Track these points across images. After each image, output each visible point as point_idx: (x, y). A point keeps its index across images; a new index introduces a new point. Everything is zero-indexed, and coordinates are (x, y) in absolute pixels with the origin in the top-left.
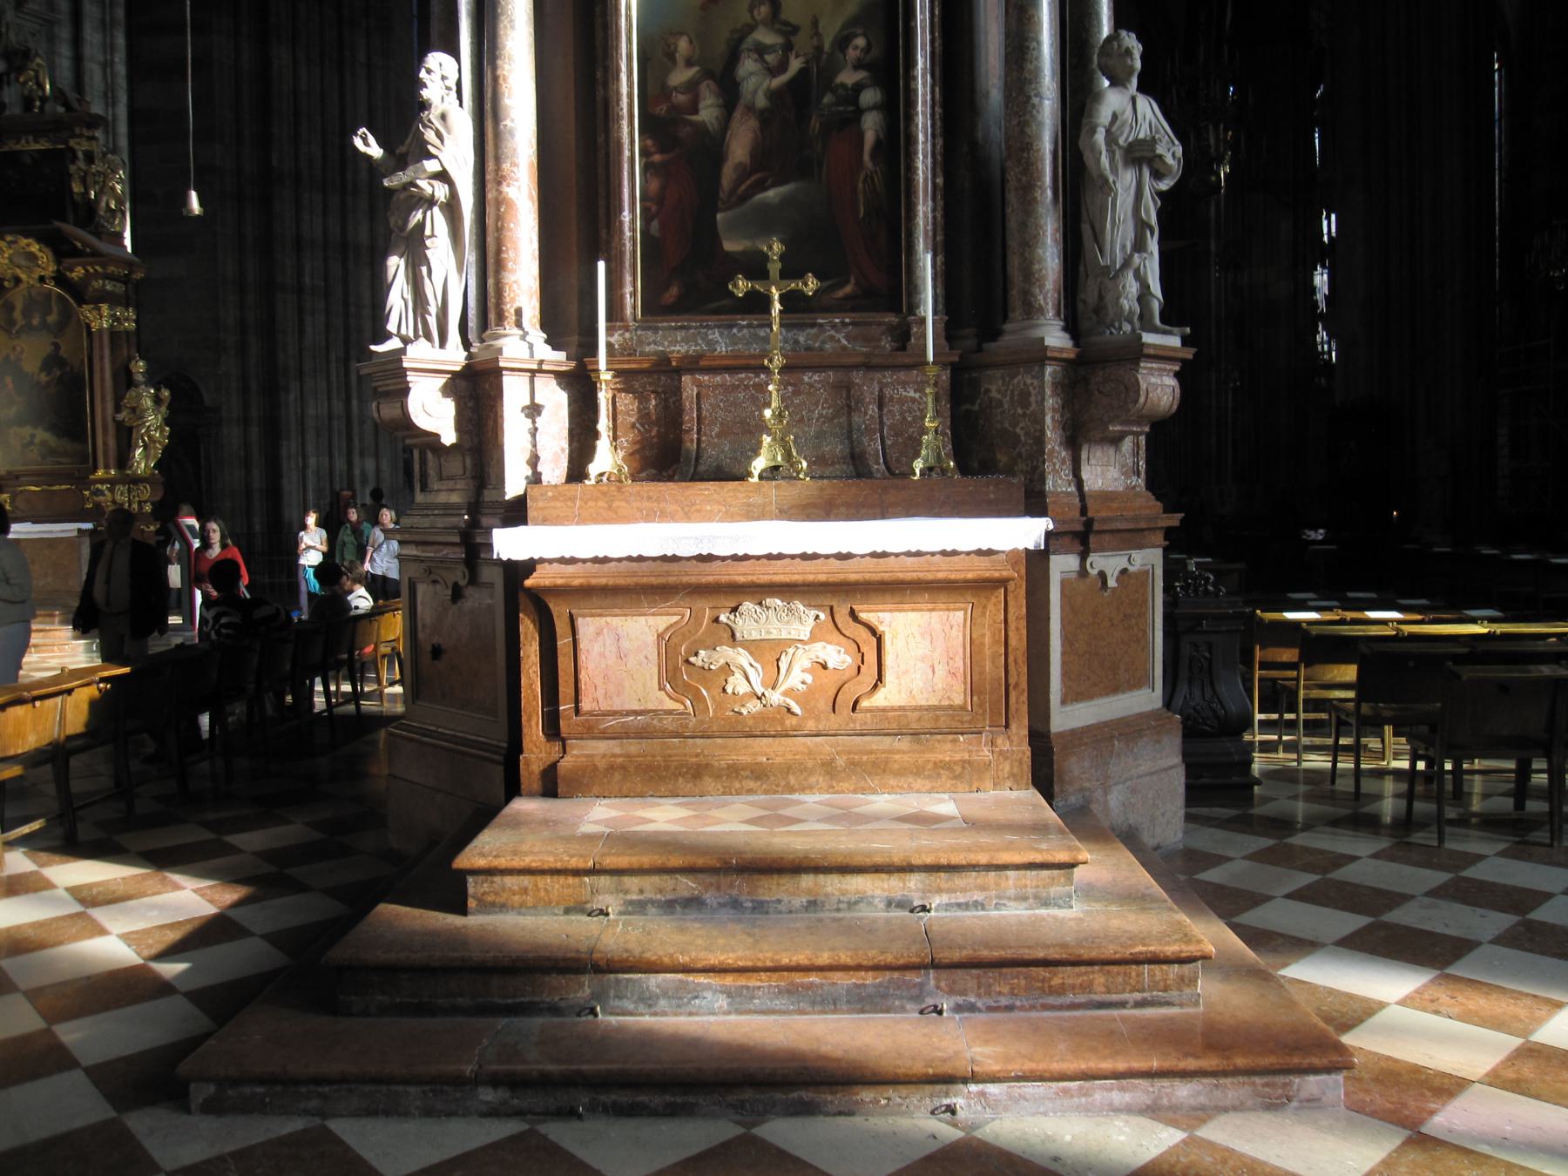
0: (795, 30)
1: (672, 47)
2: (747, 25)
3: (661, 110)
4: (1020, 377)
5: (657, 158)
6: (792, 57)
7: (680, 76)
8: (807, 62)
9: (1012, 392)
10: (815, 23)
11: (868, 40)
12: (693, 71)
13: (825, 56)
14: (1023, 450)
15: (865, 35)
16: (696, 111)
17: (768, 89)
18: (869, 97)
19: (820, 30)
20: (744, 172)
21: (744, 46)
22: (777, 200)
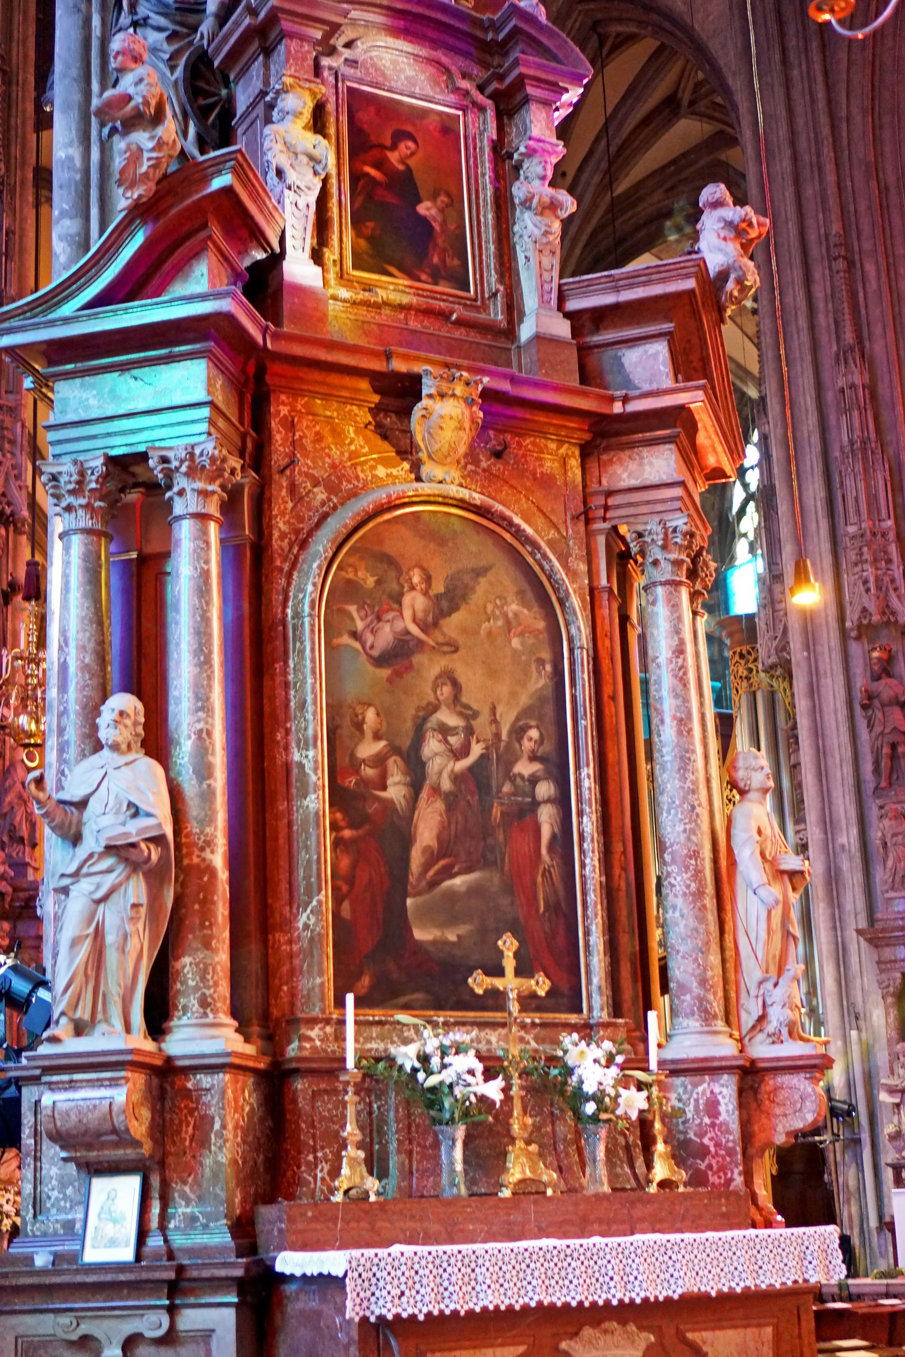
0: (475, 715)
1: (360, 717)
2: (429, 704)
3: (351, 782)
4: (705, 1085)
5: (347, 833)
6: (474, 741)
7: (368, 749)
8: (487, 748)
9: (697, 1101)
10: (493, 710)
11: (541, 735)
12: (382, 744)
13: (503, 744)
14: (714, 1162)
15: (538, 727)
16: (384, 788)
17: (452, 771)
18: (544, 789)
19: (498, 717)
20: (432, 857)
21: (429, 725)
22: (463, 889)
